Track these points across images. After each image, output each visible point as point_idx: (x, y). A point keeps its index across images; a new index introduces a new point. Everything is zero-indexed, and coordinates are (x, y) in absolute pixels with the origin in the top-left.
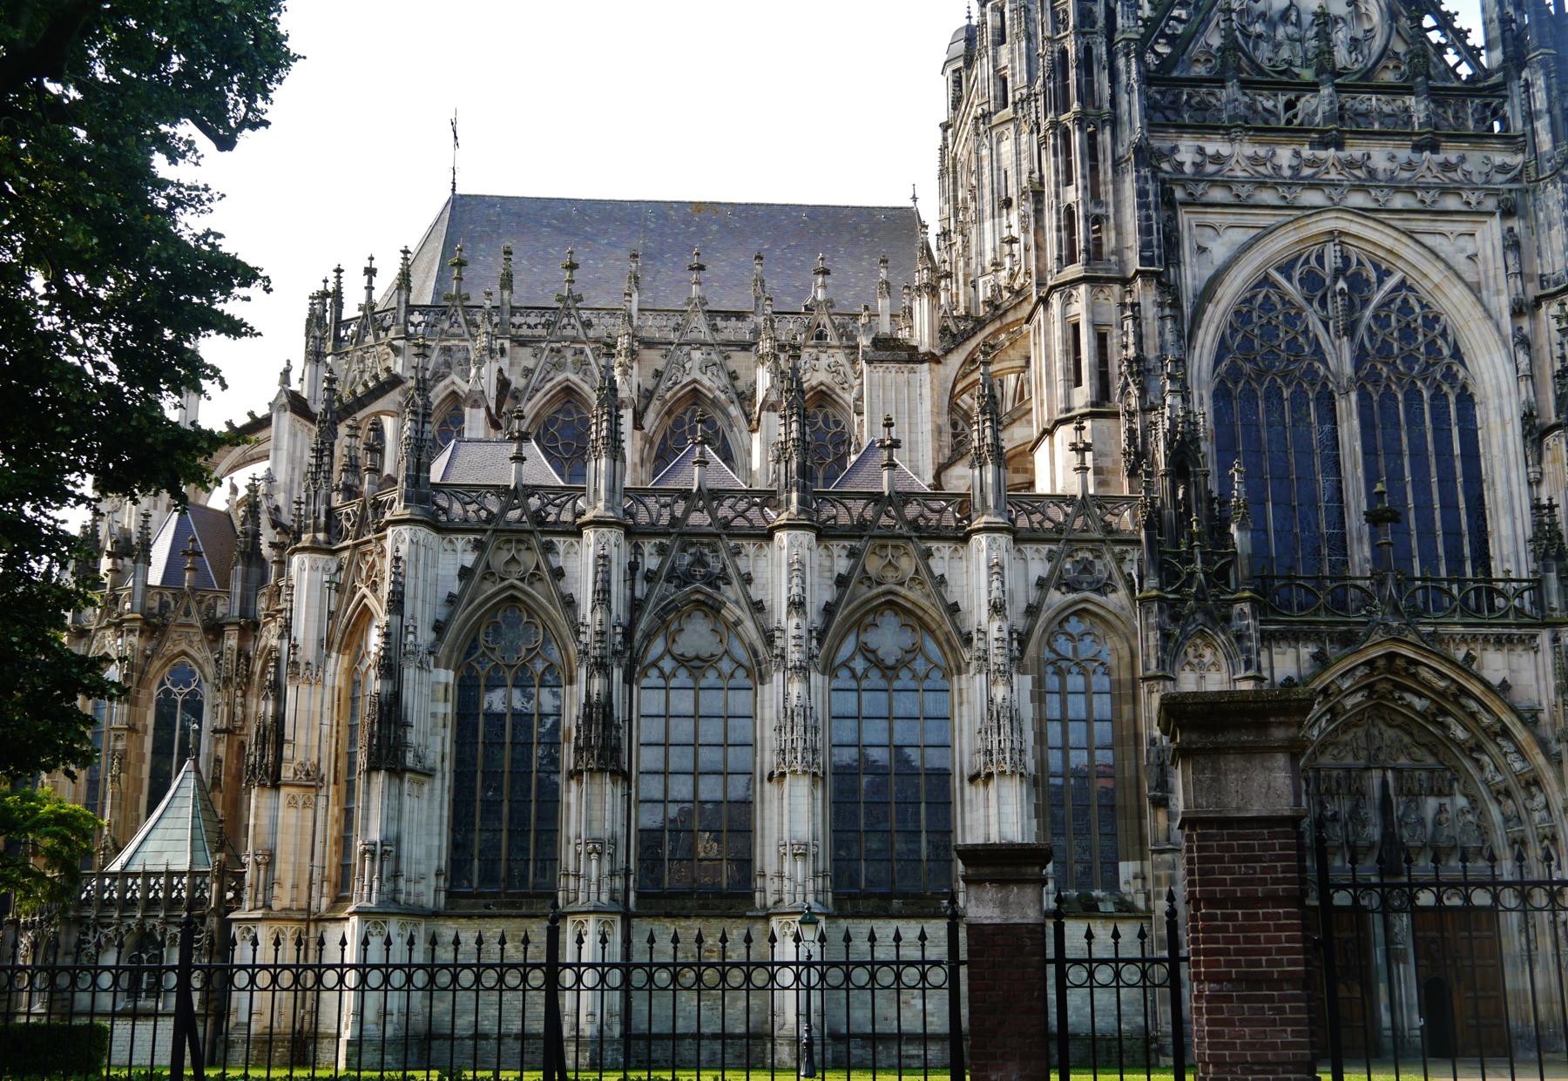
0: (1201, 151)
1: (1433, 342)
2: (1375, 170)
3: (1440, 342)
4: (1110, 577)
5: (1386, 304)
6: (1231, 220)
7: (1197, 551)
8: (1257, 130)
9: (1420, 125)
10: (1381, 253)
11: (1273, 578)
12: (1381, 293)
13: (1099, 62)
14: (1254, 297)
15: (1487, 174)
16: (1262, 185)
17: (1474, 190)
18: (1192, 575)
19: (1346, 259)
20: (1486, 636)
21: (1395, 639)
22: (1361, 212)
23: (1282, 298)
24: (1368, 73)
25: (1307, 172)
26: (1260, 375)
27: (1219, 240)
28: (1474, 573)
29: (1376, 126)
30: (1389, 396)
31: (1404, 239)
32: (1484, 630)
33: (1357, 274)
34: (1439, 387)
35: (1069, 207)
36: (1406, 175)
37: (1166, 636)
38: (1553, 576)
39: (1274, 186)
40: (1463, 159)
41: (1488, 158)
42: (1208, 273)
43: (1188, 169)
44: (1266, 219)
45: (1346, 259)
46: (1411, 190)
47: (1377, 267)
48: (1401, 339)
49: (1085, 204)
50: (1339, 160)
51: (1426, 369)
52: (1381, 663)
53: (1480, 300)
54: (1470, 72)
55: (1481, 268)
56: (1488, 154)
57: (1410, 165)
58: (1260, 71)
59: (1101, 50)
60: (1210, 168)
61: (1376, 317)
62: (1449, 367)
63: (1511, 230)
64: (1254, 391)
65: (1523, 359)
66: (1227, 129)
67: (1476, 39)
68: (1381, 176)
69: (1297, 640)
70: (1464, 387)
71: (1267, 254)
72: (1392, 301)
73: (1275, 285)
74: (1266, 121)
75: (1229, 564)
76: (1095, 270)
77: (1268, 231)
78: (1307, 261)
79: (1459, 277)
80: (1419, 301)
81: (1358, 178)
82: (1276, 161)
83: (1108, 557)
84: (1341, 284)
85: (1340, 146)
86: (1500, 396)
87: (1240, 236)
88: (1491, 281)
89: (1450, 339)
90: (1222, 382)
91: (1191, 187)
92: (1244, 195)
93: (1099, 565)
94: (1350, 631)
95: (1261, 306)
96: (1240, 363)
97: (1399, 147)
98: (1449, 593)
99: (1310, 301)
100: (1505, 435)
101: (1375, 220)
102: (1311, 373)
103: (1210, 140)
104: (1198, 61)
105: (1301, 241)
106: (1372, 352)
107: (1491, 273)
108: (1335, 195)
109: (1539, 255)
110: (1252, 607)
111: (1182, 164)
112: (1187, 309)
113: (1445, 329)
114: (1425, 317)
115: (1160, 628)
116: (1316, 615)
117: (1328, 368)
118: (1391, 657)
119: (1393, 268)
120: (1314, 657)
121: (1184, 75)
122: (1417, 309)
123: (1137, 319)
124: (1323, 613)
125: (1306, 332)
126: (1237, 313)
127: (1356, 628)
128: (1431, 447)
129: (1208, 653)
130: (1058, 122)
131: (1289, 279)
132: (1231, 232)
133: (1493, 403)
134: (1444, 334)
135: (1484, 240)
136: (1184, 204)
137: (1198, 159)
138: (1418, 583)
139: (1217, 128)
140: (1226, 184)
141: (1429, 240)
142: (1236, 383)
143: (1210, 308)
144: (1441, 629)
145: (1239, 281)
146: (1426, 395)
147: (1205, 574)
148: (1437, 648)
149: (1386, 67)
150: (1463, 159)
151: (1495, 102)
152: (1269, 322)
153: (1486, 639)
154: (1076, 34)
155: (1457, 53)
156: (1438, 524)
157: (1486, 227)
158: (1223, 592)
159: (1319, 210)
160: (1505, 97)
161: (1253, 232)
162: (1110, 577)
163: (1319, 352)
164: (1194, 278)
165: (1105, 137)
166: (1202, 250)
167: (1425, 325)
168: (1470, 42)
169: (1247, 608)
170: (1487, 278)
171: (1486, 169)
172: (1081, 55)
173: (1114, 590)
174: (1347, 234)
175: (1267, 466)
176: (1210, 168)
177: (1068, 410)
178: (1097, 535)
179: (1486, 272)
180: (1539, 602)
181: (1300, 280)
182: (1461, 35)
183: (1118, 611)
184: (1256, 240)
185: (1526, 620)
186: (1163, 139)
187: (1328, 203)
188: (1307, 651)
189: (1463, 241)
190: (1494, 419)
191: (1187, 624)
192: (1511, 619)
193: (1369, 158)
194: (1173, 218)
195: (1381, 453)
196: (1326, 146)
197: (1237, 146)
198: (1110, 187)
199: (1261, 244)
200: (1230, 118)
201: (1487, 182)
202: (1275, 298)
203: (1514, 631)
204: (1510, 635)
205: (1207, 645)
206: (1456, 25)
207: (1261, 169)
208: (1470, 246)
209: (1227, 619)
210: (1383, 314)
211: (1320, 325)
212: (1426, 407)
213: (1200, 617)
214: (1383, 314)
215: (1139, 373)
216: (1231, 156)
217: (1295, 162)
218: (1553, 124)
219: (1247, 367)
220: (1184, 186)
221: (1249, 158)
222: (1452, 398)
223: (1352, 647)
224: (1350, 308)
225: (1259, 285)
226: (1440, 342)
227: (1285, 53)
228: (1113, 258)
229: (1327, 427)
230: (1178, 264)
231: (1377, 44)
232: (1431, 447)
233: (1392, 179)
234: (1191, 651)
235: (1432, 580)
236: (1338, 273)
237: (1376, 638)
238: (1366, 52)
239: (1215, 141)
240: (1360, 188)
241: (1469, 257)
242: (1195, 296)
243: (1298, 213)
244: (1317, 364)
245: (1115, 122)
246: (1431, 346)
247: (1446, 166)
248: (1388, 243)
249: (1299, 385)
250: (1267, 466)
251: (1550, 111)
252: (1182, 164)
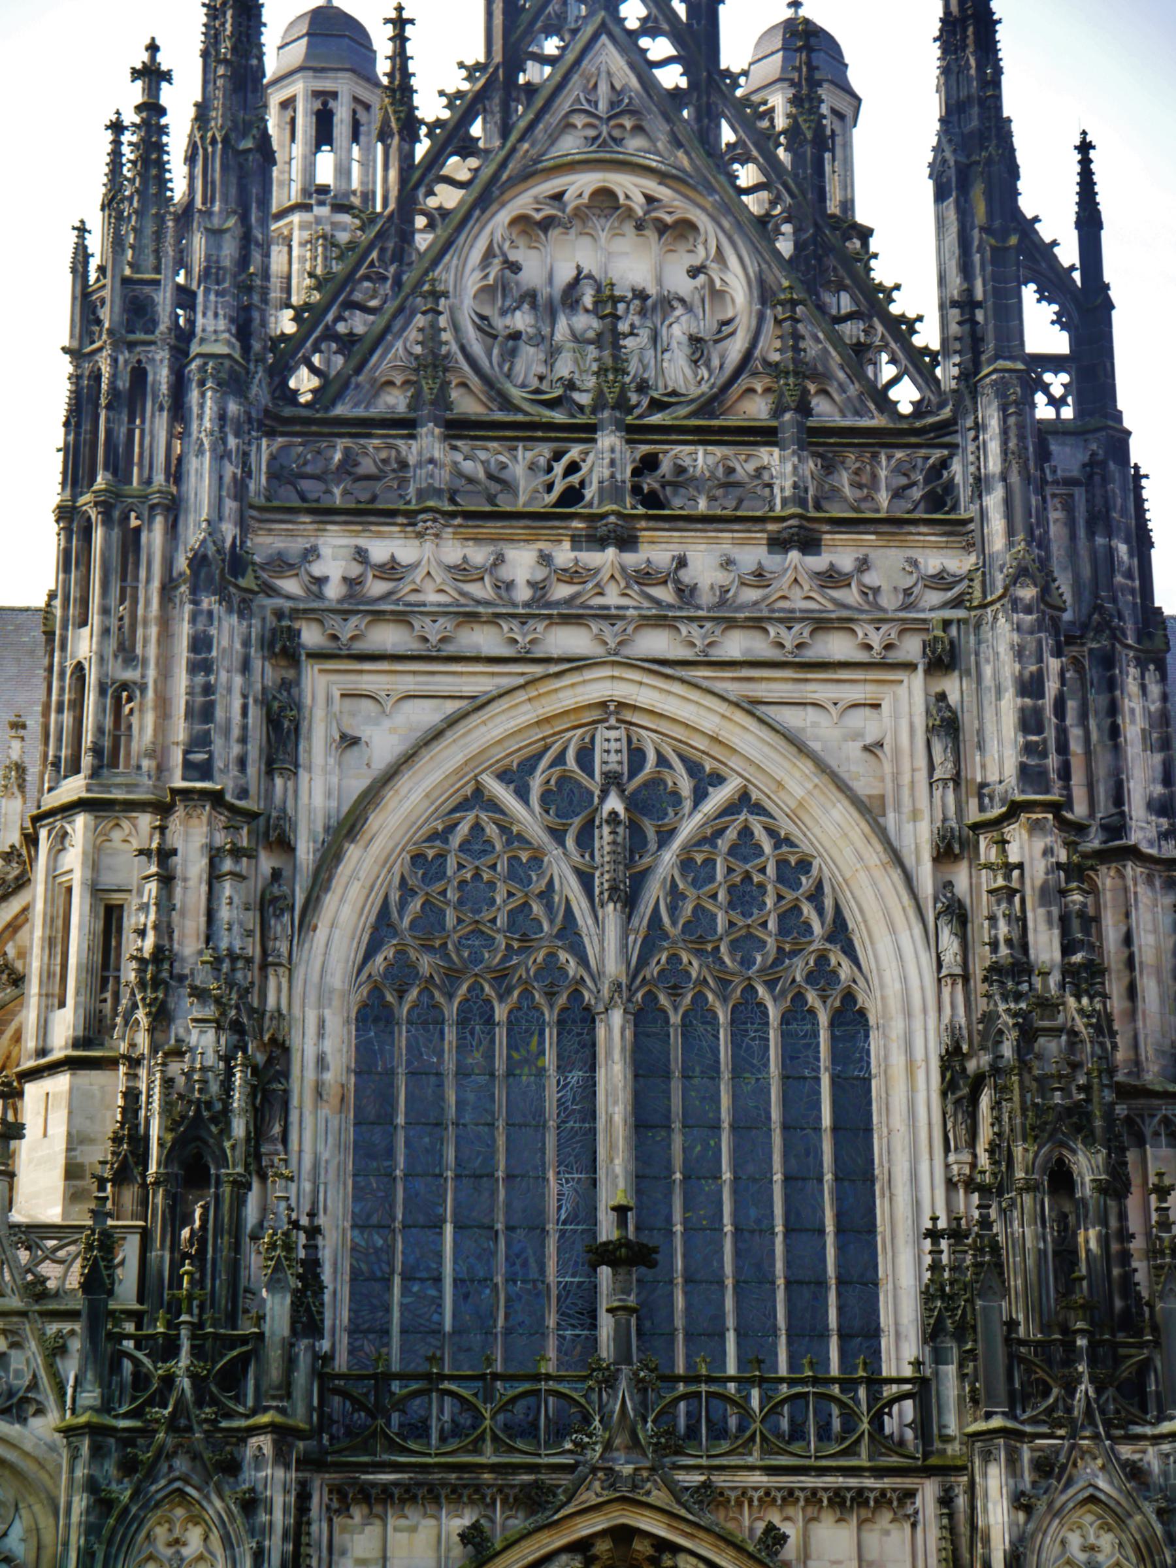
0: (361, 555)
1: (796, 909)
2: (694, 589)
3: (807, 909)
4: (34, 1385)
5: (707, 839)
6: (409, 684)
7: (184, 1332)
8: (468, 515)
9: (785, 502)
10: (701, 743)
11: (389, 1377)
12: (698, 818)
13: (155, 396)
14: (451, 828)
15: (907, 592)
16: (471, 618)
17: (878, 622)
18: (169, 1381)
19: (636, 756)
20: (814, 1492)
21: (623, 1499)
22: (660, 666)
23: (504, 829)
24: (710, 404)
25: (562, 591)
26: (453, 976)
27: (386, 723)
28: (792, 1367)
29: (702, 506)
30: (700, 1014)
31: (739, 716)
32: (810, 1481)
33: (656, 782)
34: (799, 997)
35: (79, 667)
36: (751, 595)
37: (102, 1502)
38: (951, 1370)
39: (495, 619)
40: (863, 565)
41: (914, 563)
42: (357, 785)
43: (334, 591)
44: (479, 682)
45: (636, 756)
46: (757, 624)
47: (693, 768)
48: (731, 905)
49: (102, 659)
50: (623, 569)
51: (778, 961)
52: (602, 1547)
53: (881, 833)
54: (916, 396)
55: (888, 768)
56: (910, 553)
57: (760, 577)
58: (506, 403)
59: (161, 376)
60: (377, 588)
61: (686, 864)
62: (822, 958)
63: (942, 697)
64: (436, 1007)
65: (949, 943)
66: (411, 515)
67: (928, 336)
68: (706, 598)
69: (436, 1500)
70: (849, 997)
71: (474, 748)
72: (720, 832)
73: (493, 806)
74: (491, 499)
75: (243, 1362)
76: (107, 788)
77: (480, 704)
78: (560, 759)
79: (842, 786)
80: (771, 832)
81: (657, 602)
82: (505, 573)
83: (33, 1345)
84: (614, 803)
85: (627, 543)
86: (908, 1014)
87: (427, 715)
88: (906, 792)
89: (828, 903)
90: (376, 991)
91: (334, 623)
92: (434, 639)
93: (17, 1360)
94: (536, 1484)
95: (464, 847)
96: (413, 955)
97: (743, 543)
98: (742, 1405)
99: (558, 835)
100: (912, 1089)
101: (683, 681)
102: (551, 970)
103: (380, 535)
104: (390, 383)
105: (547, 720)
106: (674, 931)
107: (906, 779)
108: (611, 635)
109: (981, 746)
110: (276, 1444)
111: (321, 581)
112: (306, 852)
113: (819, 886)
114: (782, 863)
115: (92, 1486)
116: (477, 1451)
117: (583, 961)
118: (623, 1535)
119: (724, 770)
120: (465, 1537)
121: (360, 412)
122: (767, 847)
123: (167, 880)
124: (488, 1447)
125: (546, 894)
126: (417, 859)
127: (546, 1478)
128: (775, 1114)
129: (194, 1536)
130: (74, 508)
131: (522, 794)
132: (409, 706)
133: (897, 1027)
134: (816, 896)
135: (896, 716)
136: (318, 656)
137: (355, 570)
138: (681, 1388)
139: (393, 513)
140: (402, 618)
141: (790, 718)
142: (401, 994)
143: (353, 852)
144: (719, 1480)
145: (416, 796)
146: (774, 1013)
147: (193, 1377)
148: (707, 1519)
149: (752, 391)
150: (863, 565)
151: (937, 454)
152: (477, 876)
153: (813, 1497)
154: (115, 346)
155: (893, 361)
156: (779, 1266)
157: (902, 691)
158: (230, 1415)
159: (577, 664)
160: (954, 446)
161: (451, 707)
162: (34, 1385)
163: (569, 931)
164: (329, 795)
165: (154, 538)
166: (349, 742)
167: (781, 879)
168: (918, 341)
169: (264, 1443)
170: (898, 787)
171: (908, 582)
172: (123, 384)
173: (40, 1411)
174: (635, 708)
175: (450, 1155)
176: (377, 588)
177: (42, 1052)
178: (15, 1302)
179: (896, 776)
180: (924, 1424)
181: (545, 798)
182: (903, 328)
183: (40, 1453)
184: (452, 722)
185: (894, 1460)
186: (291, 534)
187: (597, 650)
188: (458, 1522)
189: (857, 719)
190: (898, 1060)
191: (151, 1475)
192: (863, 1461)
193: (682, 562)
194: (288, 685)
195: (677, 1125)
196: (601, 543)
197: (429, 546)
198: (153, 631)
199: (461, 728)
200: (421, 494)
201: (905, 607)
202: (492, 831)
203: (869, 1482)
204: (860, 1491)
205: (195, 1520)
206: (895, 309)
207: (475, 589)
208: (870, 726)
209: (232, 1467)
210: (699, 858)
211: (573, 881)
212: (772, 1035)
213: (181, 1464)
214: (699, 858)
215: (156, 983)
216: (414, 566)
217: (540, 574)
218: (1008, 502)
219: (426, 963)
220: (320, 622)
221: (449, 568)
222: (823, 1019)
223: (540, 1518)
224: (635, 843)
225: (464, 805)
226: (807, 909)
227: (564, 367)
228: (146, 764)
229: (575, 1076)
230: (293, 769)
231: (735, 348)
232: (775, 1114)
233: (722, 603)
234: (161, 1532)
235: (710, 1380)
236: (612, 780)
237: (588, 1497)
238: (716, 362)
239: (390, 536)
240: (661, 620)
241: (867, 749)
242: (327, 829)
243: (538, 670)
244: (563, 956)
245: (174, 508)
246: (790, 919)
247: (831, 578)
248: (709, 723)
249: (527, 994)
250: (450, 1155)
251: (1004, 478)
252: (321, 581)
